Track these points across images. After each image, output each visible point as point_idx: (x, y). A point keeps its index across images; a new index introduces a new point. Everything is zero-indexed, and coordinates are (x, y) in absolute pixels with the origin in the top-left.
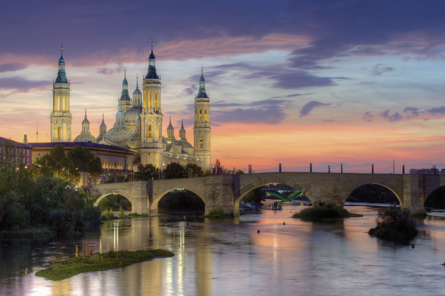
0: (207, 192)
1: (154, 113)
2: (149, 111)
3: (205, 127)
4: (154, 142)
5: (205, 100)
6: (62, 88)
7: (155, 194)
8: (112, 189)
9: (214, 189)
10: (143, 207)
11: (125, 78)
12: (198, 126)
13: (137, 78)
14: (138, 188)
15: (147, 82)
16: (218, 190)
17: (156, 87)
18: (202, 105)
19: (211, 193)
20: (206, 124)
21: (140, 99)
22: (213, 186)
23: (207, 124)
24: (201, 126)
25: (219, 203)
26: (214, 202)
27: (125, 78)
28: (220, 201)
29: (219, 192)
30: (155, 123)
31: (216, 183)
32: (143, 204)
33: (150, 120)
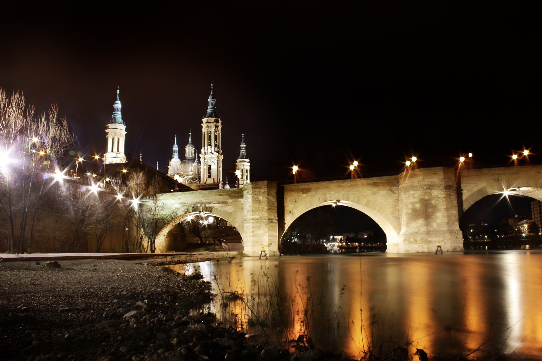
0: (407, 203)
5: (246, 161)
6: (117, 128)
7: (290, 212)
8: (199, 203)
9: (427, 197)
10: (271, 238)
14: (261, 198)
15: (207, 122)
16: (437, 198)
19: (418, 206)
22: (424, 190)
25: (439, 225)
26: (428, 224)
28: (439, 221)
29: (437, 202)
31: (429, 183)
32: (270, 232)
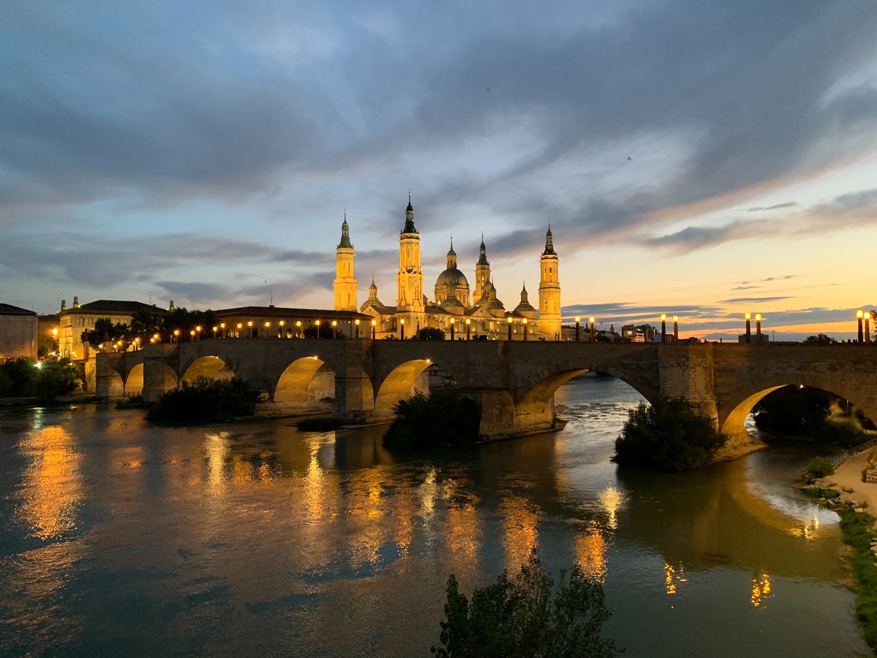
1: (406, 272)
2: (403, 271)
3: (548, 288)
4: (406, 305)
11: (483, 242)
12: (542, 287)
13: (451, 238)
17: (409, 243)
18: (546, 263)
20: (550, 284)
21: (453, 261)
23: (552, 284)
24: (545, 286)
27: (483, 242)
30: (407, 282)
33: (403, 280)
